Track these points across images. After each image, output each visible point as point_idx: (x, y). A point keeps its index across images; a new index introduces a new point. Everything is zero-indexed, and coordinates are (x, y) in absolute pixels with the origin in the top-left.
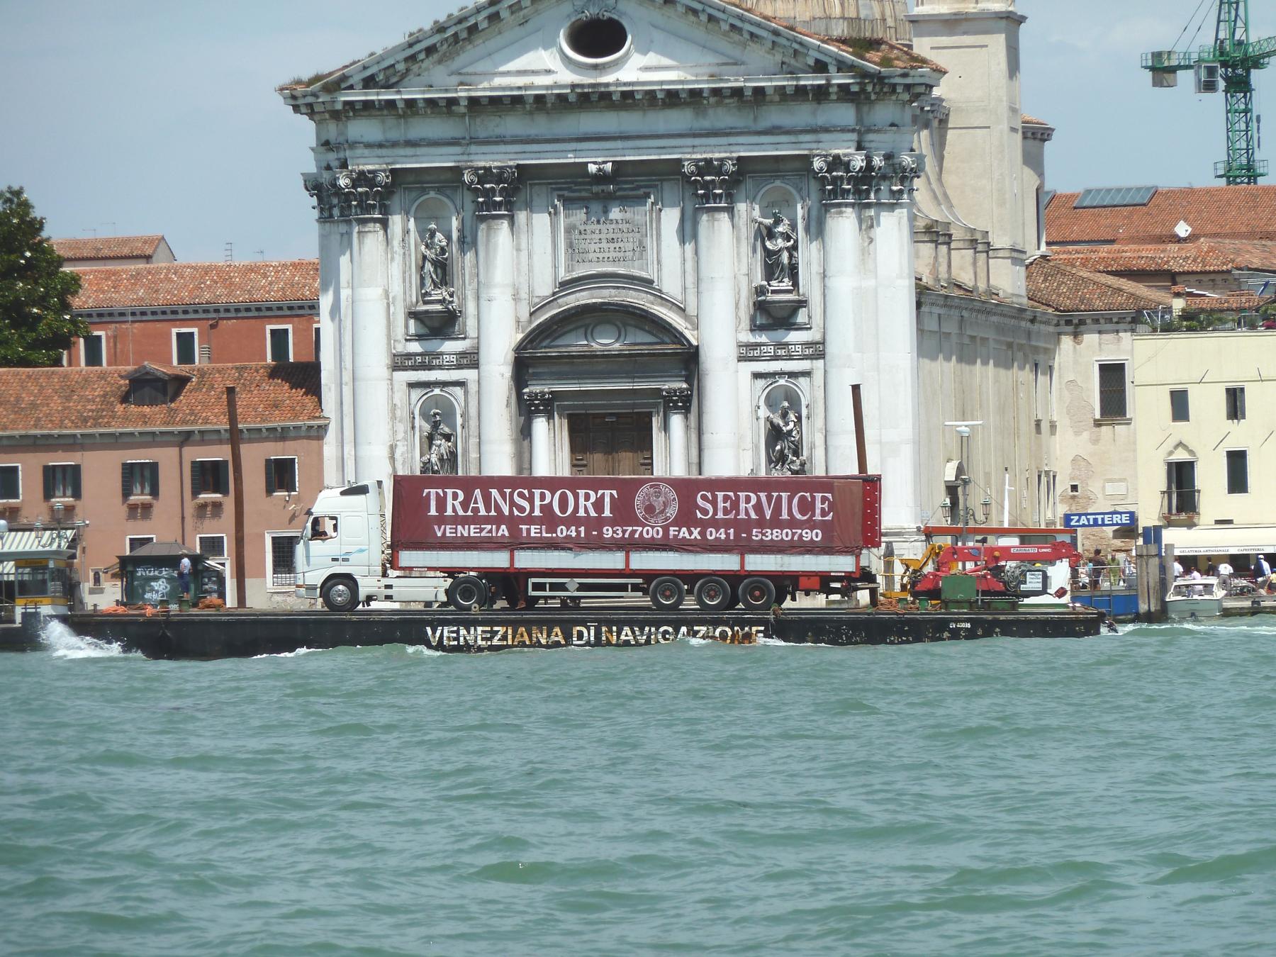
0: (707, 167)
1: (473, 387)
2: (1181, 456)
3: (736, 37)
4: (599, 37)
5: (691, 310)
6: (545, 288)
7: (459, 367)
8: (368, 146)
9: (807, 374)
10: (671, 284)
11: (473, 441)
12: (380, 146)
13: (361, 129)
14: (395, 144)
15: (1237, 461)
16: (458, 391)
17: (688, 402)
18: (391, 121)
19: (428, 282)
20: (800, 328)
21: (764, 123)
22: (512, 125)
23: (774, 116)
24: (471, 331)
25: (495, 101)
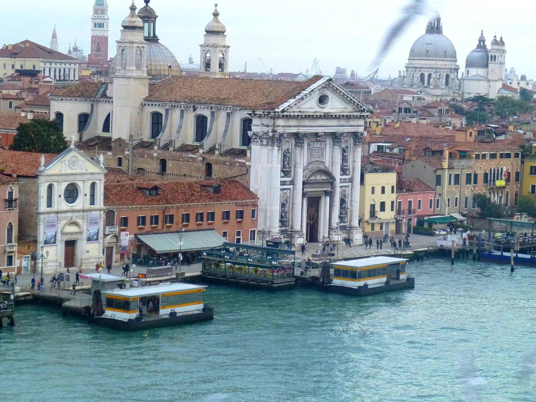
0: (342, 134)
1: (292, 190)
2: (373, 203)
3: (348, 102)
4: (322, 100)
5: (330, 171)
6: (305, 165)
7: (290, 185)
8: (282, 126)
9: (348, 186)
10: (327, 165)
11: (291, 204)
12: (284, 126)
13: (280, 122)
14: (287, 126)
15: (383, 205)
16: (289, 191)
17: (330, 194)
18: (285, 120)
19: (286, 163)
20: (348, 175)
21: (349, 124)
22: (307, 122)
23: (352, 122)
24: (292, 176)
25: (309, 116)
